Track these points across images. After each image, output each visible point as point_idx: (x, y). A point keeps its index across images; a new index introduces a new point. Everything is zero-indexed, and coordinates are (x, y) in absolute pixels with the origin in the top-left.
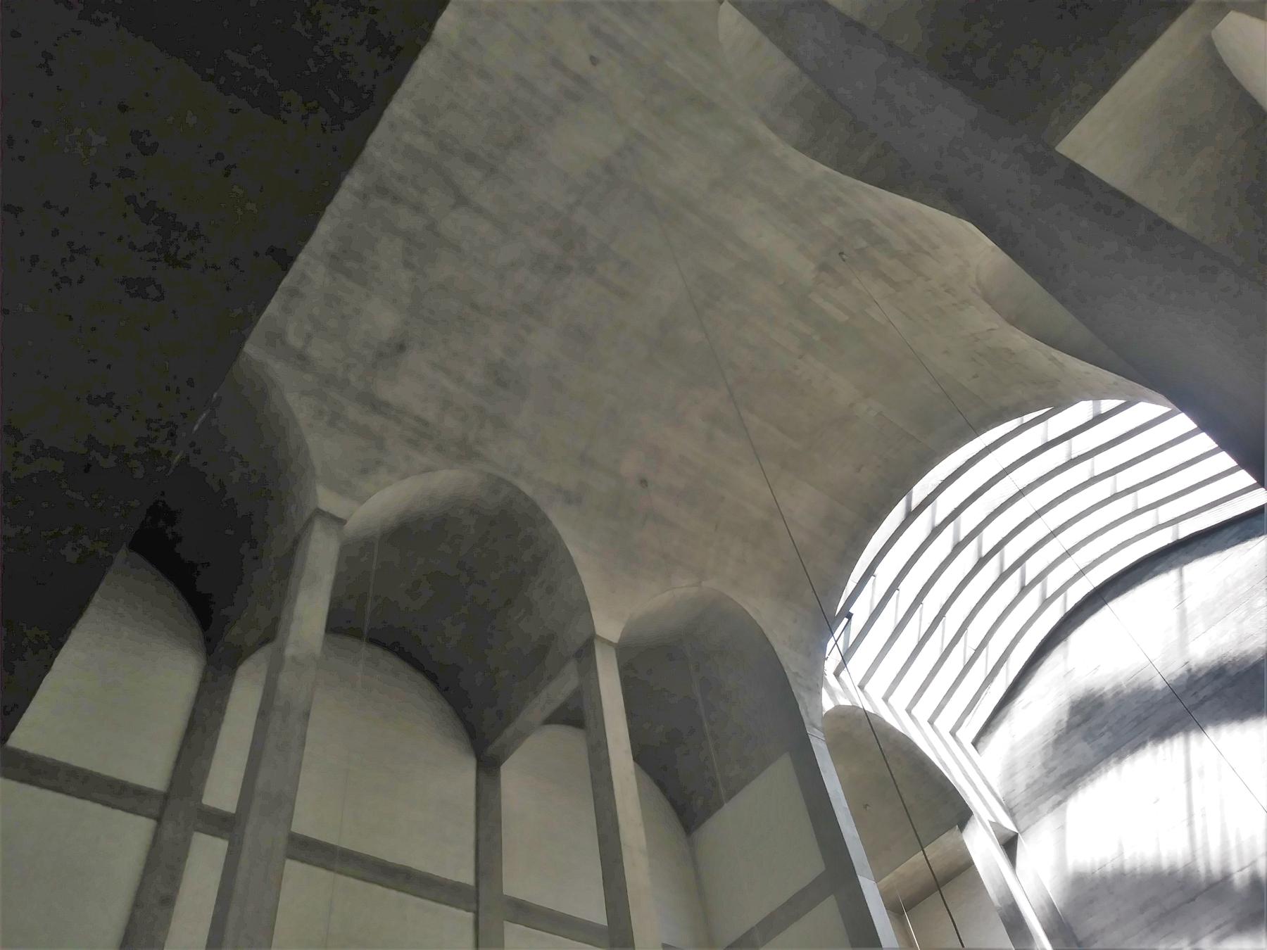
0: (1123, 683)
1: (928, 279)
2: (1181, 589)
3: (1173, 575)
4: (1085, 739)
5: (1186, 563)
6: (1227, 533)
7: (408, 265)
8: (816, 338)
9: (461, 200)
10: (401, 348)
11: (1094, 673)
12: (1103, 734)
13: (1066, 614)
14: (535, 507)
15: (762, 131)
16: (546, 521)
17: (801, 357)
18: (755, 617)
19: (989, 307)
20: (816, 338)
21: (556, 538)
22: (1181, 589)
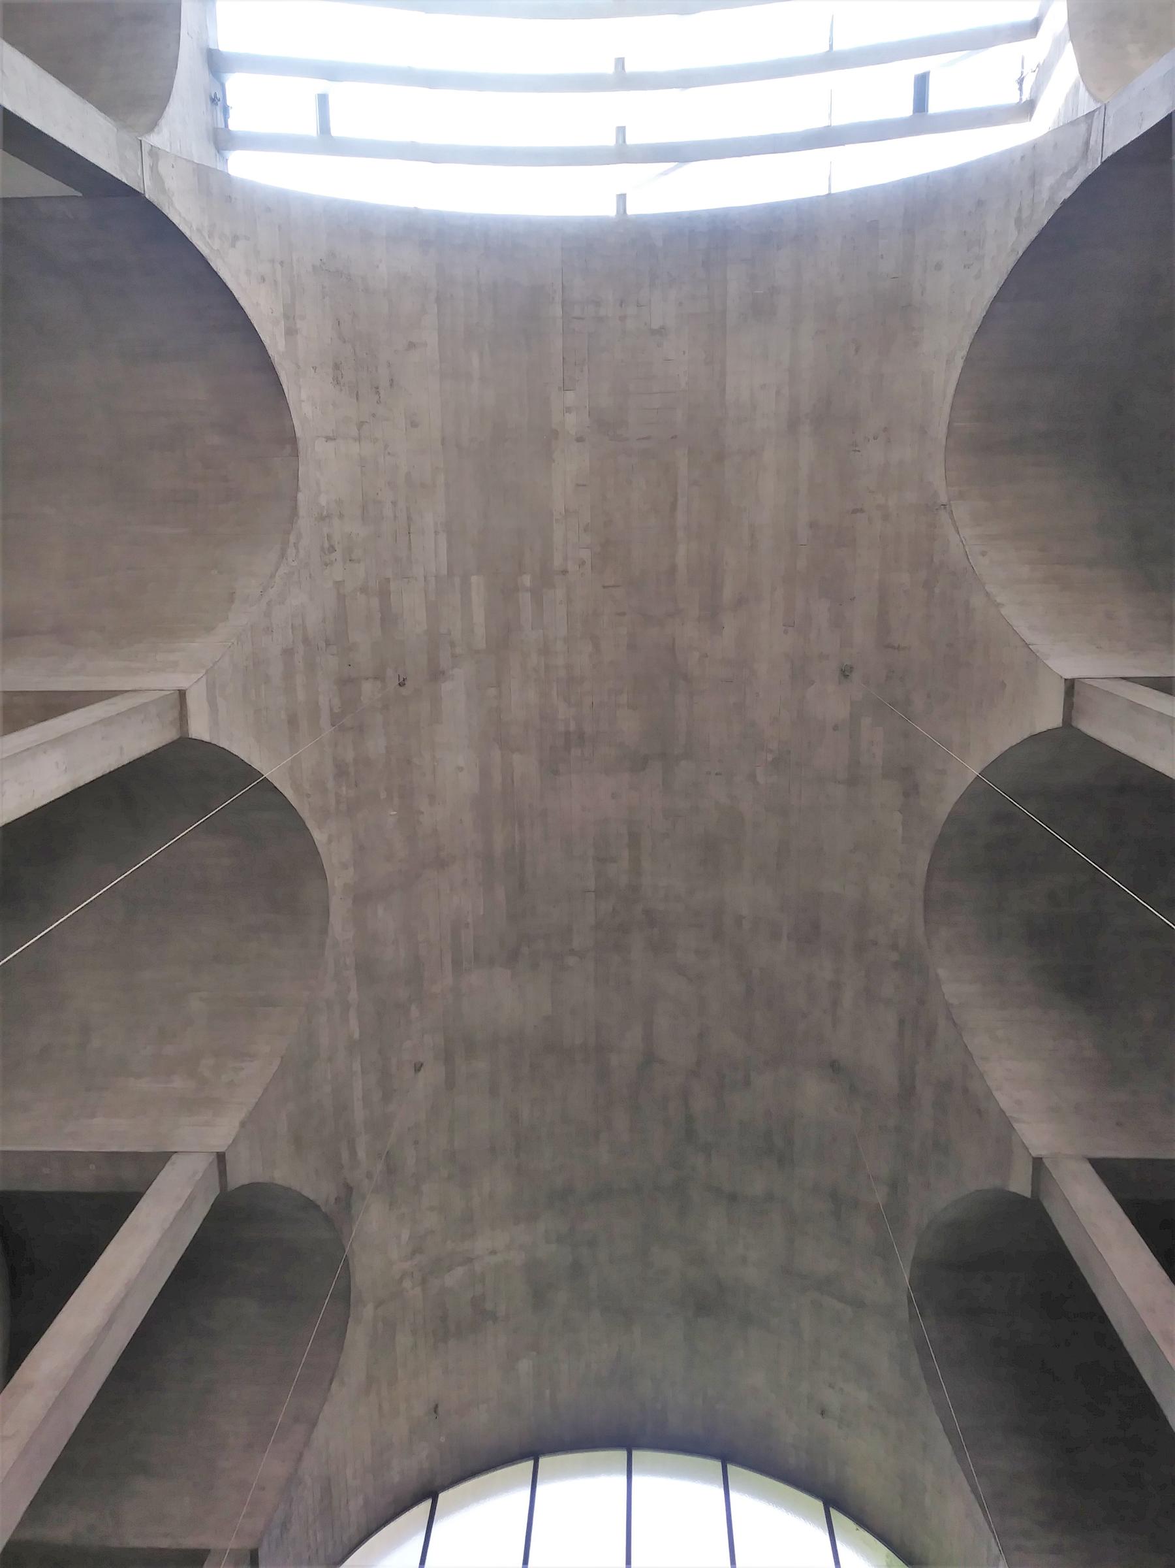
1: (338, 584)
7: (747, 1083)
8: (527, 580)
9: (649, 1058)
10: (835, 1067)
14: (942, 843)
15: (339, 908)
16: (952, 818)
17: (564, 572)
18: (959, 363)
19: (300, 496)
20: (527, 580)
21: (974, 793)
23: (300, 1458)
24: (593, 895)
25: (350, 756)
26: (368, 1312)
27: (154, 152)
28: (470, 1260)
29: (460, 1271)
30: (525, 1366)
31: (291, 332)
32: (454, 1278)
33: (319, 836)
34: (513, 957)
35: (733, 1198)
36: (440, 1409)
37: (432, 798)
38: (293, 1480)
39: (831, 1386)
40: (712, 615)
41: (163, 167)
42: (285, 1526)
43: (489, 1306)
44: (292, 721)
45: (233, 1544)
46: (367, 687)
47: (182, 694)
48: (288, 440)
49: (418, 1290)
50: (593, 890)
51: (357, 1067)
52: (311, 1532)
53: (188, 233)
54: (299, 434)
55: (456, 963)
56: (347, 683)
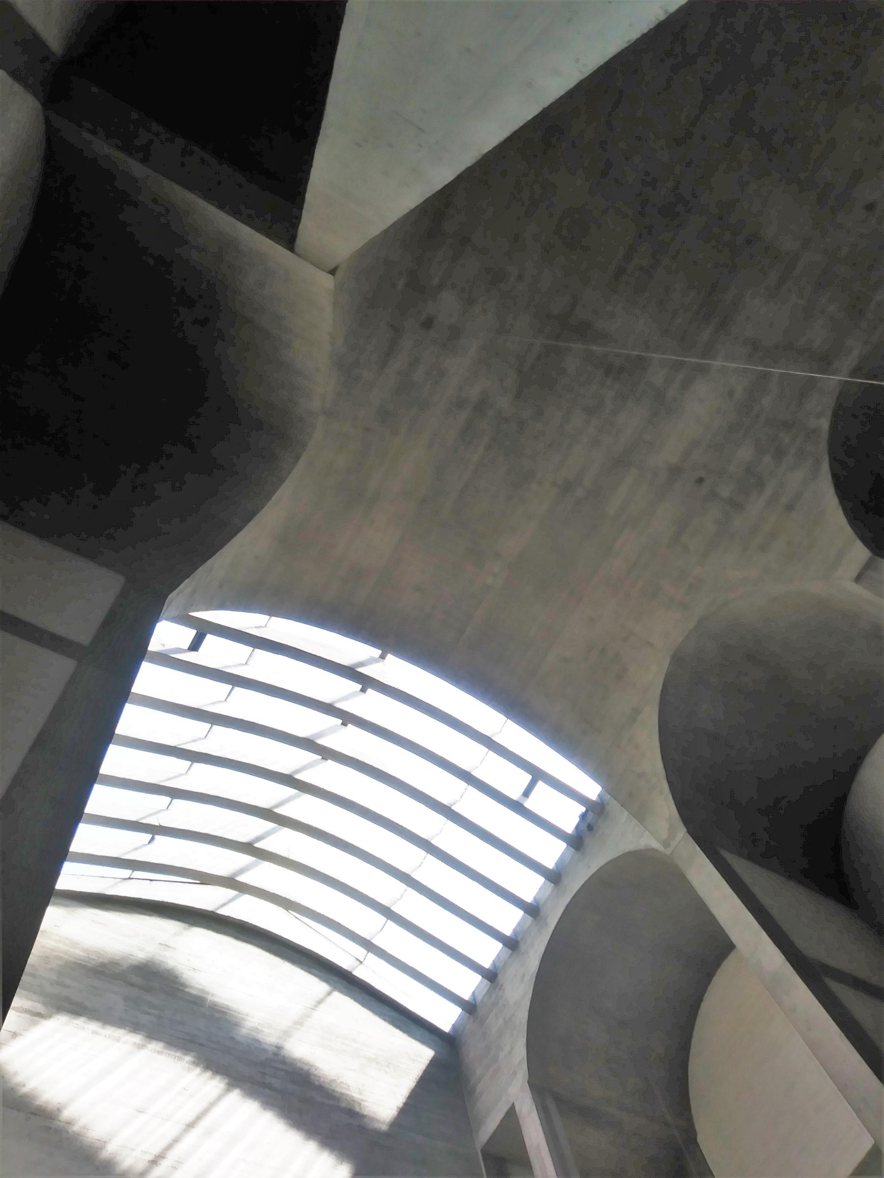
0: (208, 1001)
2: (320, 1002)
3: (323, 987)
4: (126, 999)
5: (341, 992)
6: (386, 1010)
8: (580, 493)
11: (190, 970)
12: (149, 1014)
13: (213, 912)
22: (320, 1002)
25: (767, 459)
27: (666, 844)
31: (636, 711)
33: (825, 424)
37: (731, 393)
40: (481, 406)
41: (664, 835)
44: (790, 508)
46: (725, 491)
47: (858, 579)
48: (677, 659)
53: (670, 797)
54: (668, 660)
56: (736, 505)
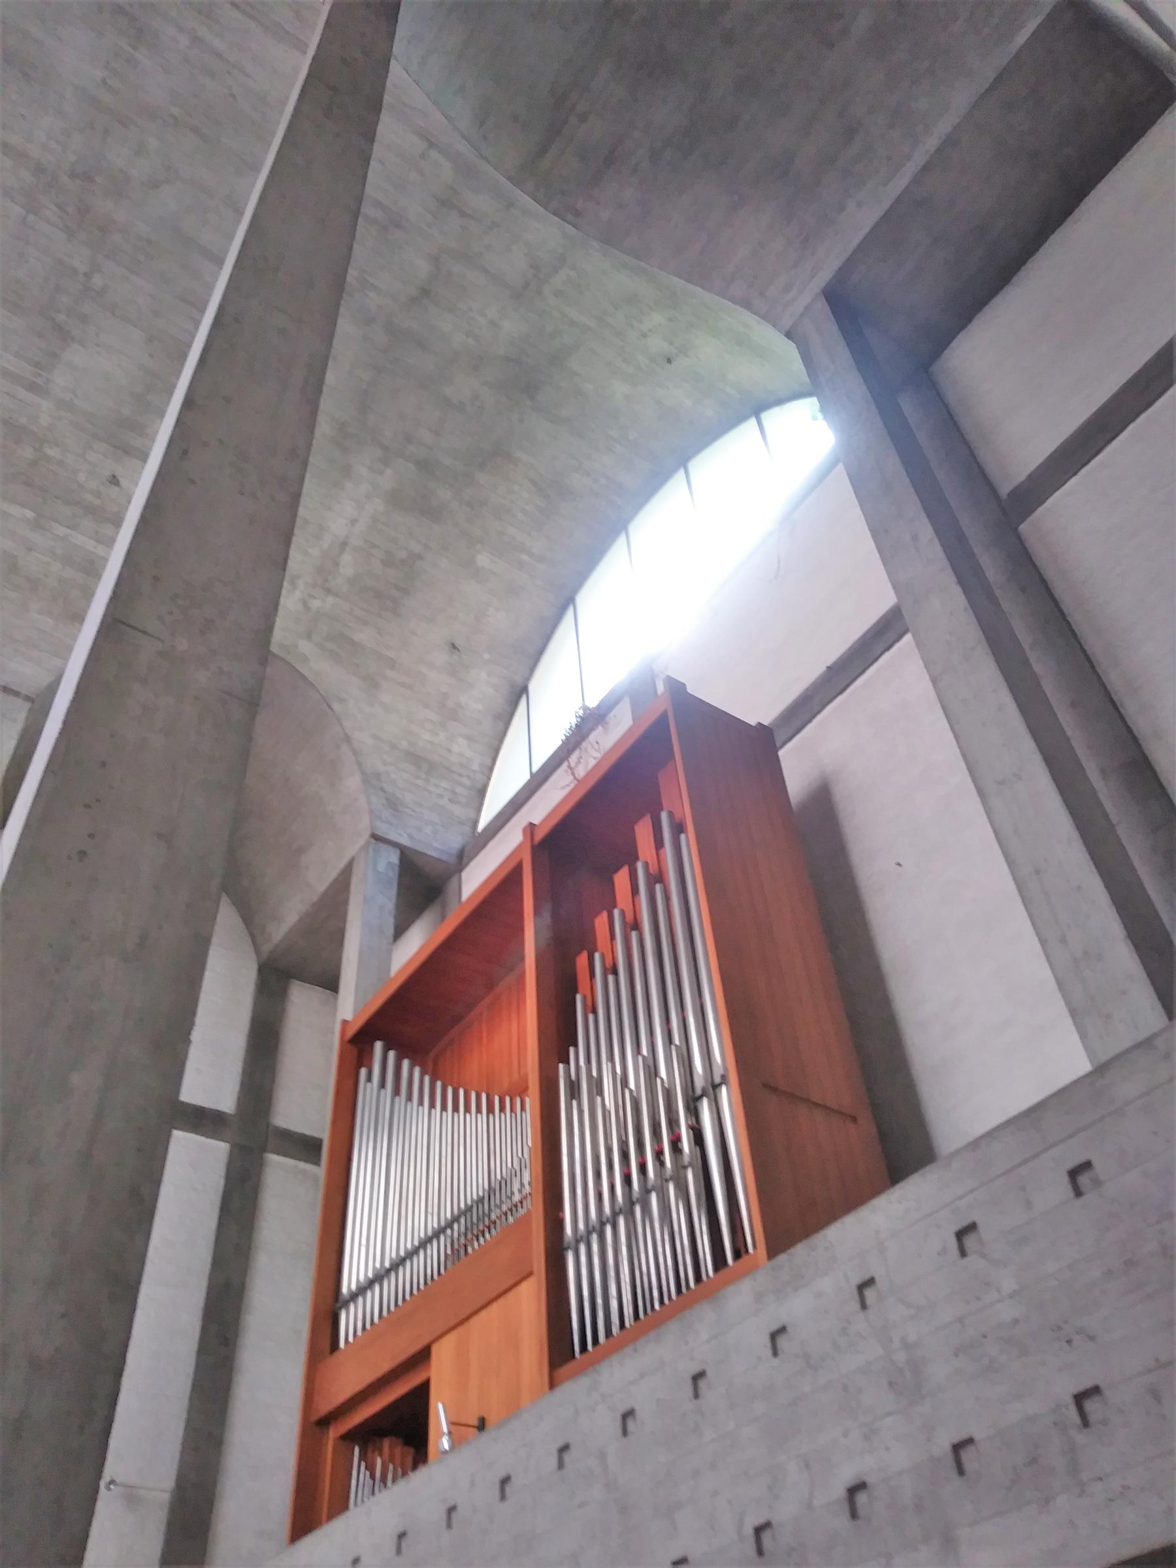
23: (359, 764)
24: (31, 217)
26: (305, 647)
28: (344, 544)
29: (347, 558)
30: (483, 560)
32: (348, 565)
34: (64, 336)
35: (425, 292)
36: (458, 643)
38: (371, 780)
39: (645, 336)
42: (394, 804)
43: (403, 554)
45: (361, 842)
49: (330, 600)
50: (24, 212)
51: (61, 531)
52: (431, 788)
55: (32, 387)
